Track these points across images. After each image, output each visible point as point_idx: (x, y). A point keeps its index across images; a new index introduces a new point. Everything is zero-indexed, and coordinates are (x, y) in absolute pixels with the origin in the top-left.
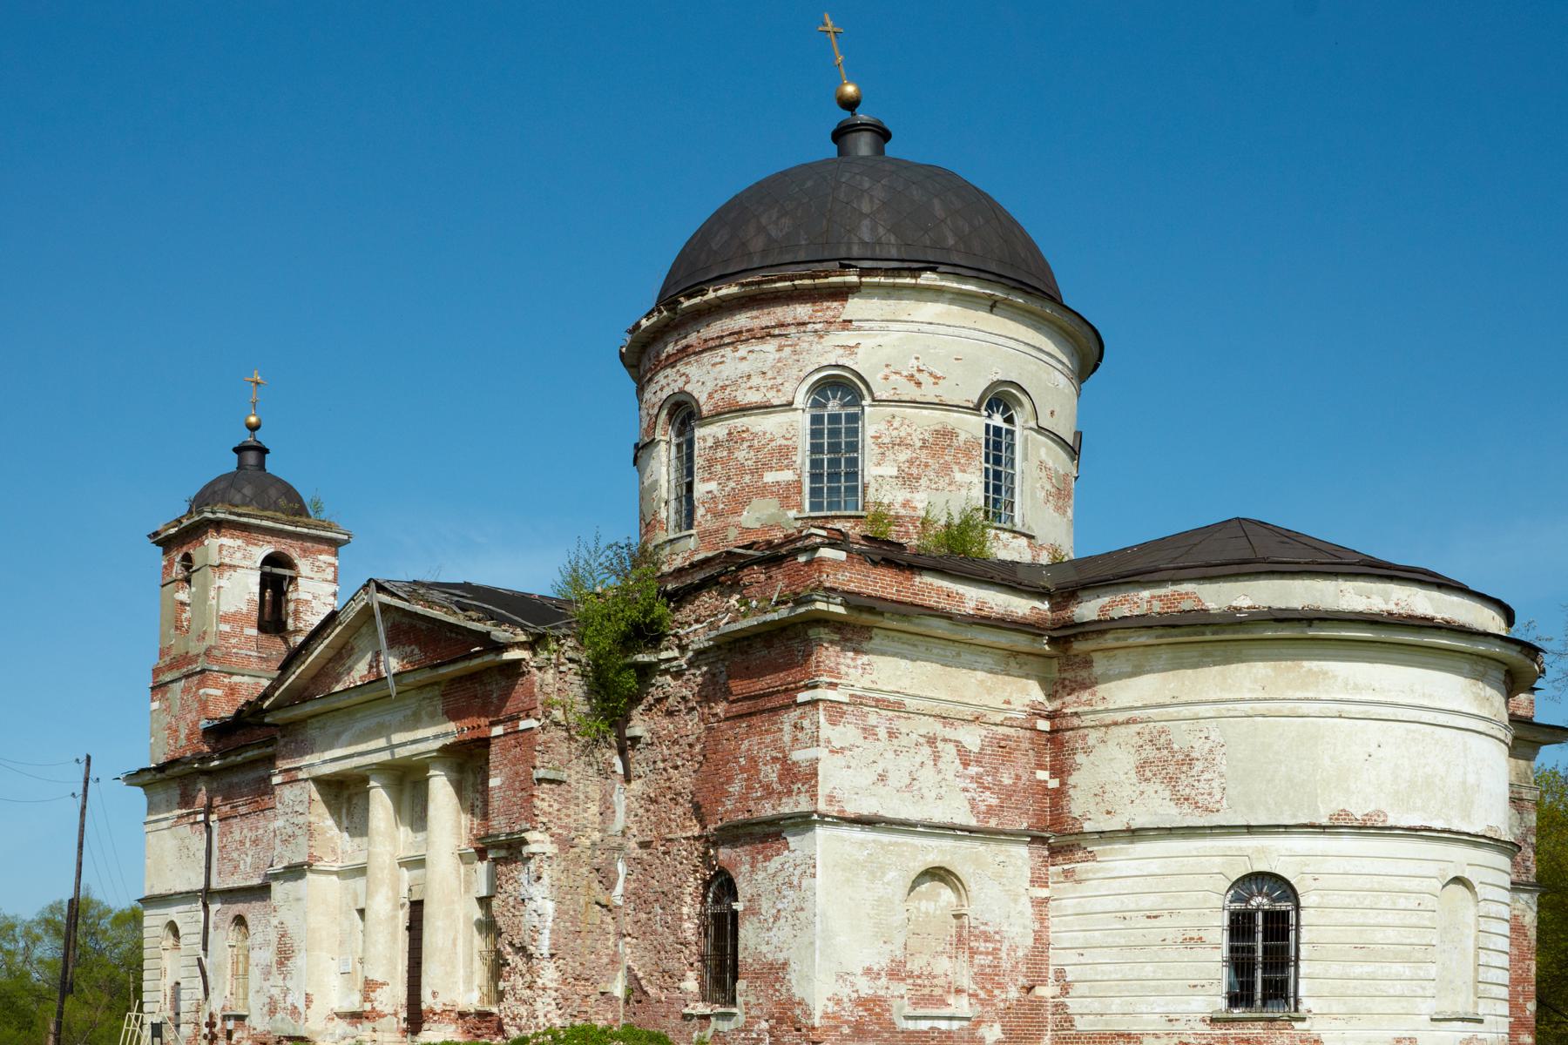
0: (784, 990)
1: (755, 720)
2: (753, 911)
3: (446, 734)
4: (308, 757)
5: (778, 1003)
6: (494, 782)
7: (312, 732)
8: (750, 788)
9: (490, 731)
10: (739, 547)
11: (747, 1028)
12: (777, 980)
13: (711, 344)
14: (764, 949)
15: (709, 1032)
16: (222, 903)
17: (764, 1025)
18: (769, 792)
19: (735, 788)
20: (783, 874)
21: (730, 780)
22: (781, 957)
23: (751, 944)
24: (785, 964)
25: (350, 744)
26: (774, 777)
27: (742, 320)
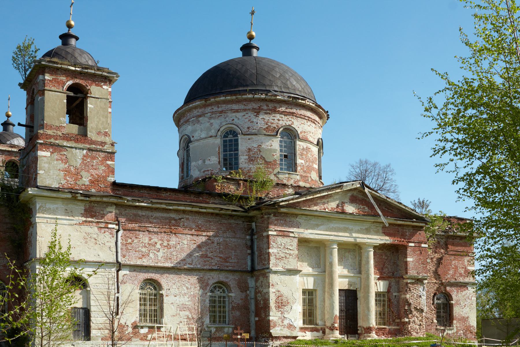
0: (467, 323)
1: (456, 257)
2: (458, 303)
3: (386, 240)
4: (295, 229)
5: (466, 326)
6: (409, 259)
7: (299, 220)
8: (455, 273)
9: (409, 244)
10: (396, 202)
11: (457, 332)
12: (465, 321)
13: (302, 116)
14: (462, 313)
15: (445, 333)
16: (130, 271)
17: (462, 332)
18: (461, 275)
19: (451, 272)
20: (467, 296)
21: (449, 270)
22: (466, 316)
23: (458, 311)
24: (468, 317)
25: (327, 231)
26: (463, 272)
27: (309, 114)
